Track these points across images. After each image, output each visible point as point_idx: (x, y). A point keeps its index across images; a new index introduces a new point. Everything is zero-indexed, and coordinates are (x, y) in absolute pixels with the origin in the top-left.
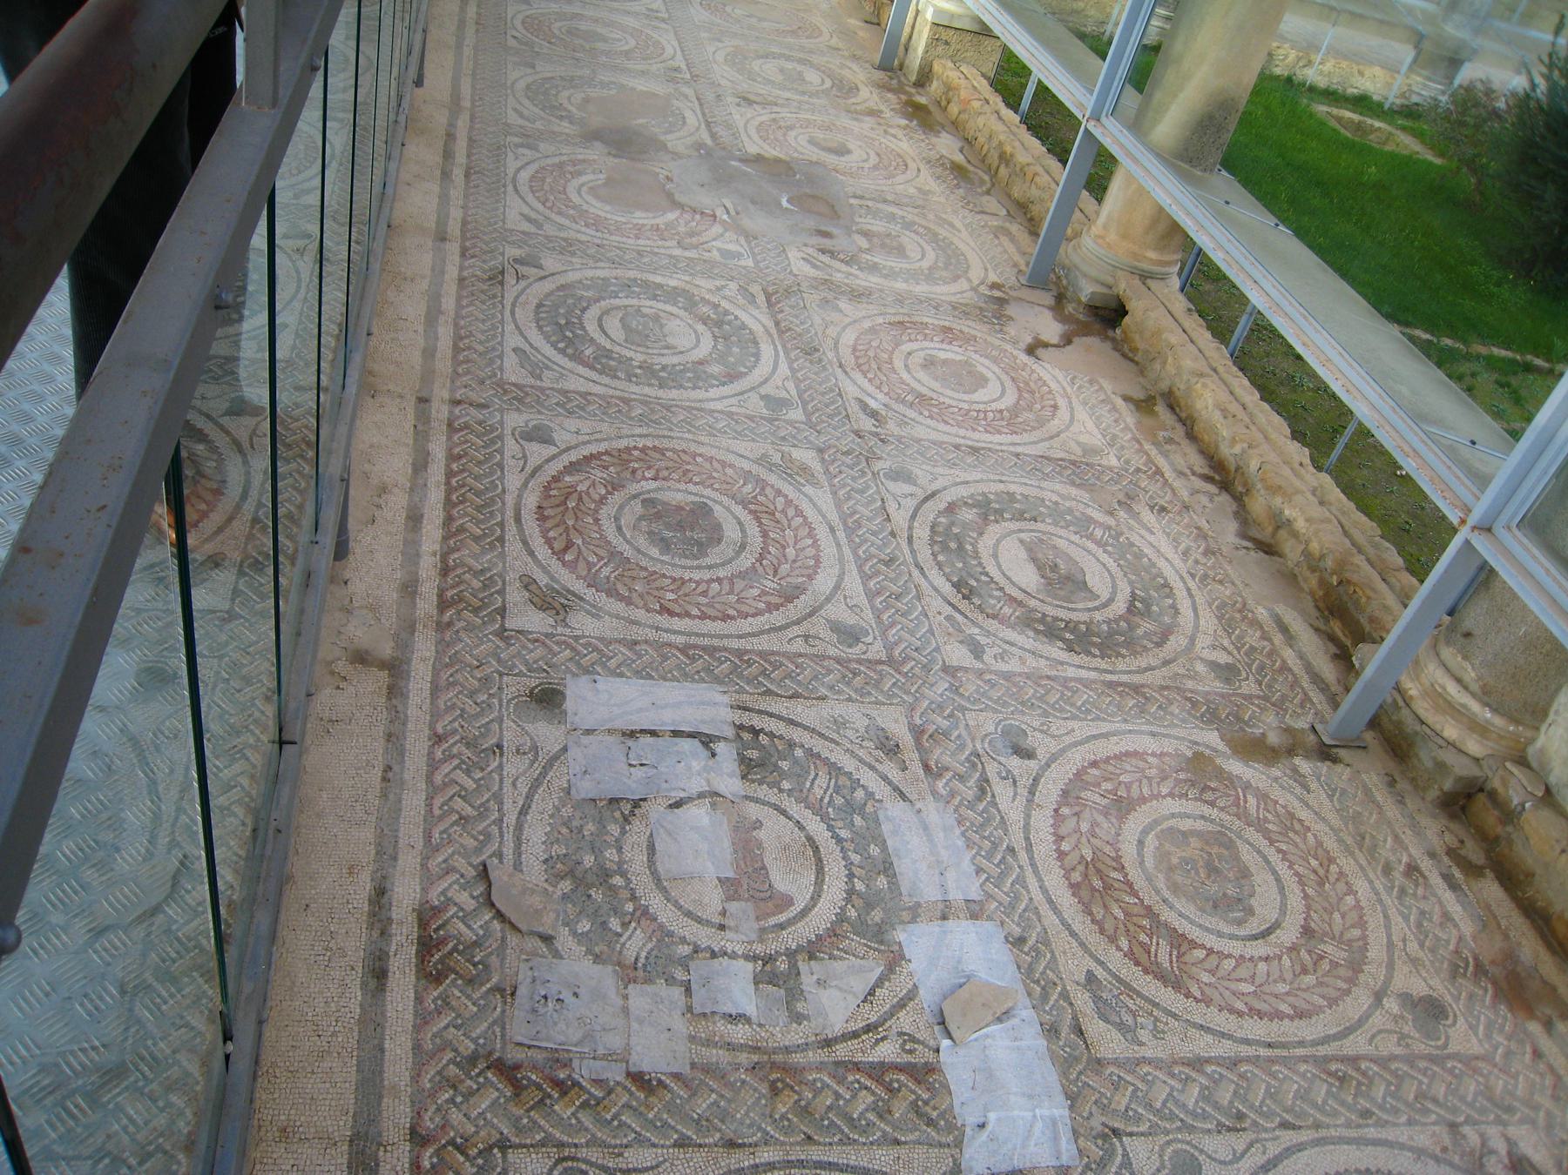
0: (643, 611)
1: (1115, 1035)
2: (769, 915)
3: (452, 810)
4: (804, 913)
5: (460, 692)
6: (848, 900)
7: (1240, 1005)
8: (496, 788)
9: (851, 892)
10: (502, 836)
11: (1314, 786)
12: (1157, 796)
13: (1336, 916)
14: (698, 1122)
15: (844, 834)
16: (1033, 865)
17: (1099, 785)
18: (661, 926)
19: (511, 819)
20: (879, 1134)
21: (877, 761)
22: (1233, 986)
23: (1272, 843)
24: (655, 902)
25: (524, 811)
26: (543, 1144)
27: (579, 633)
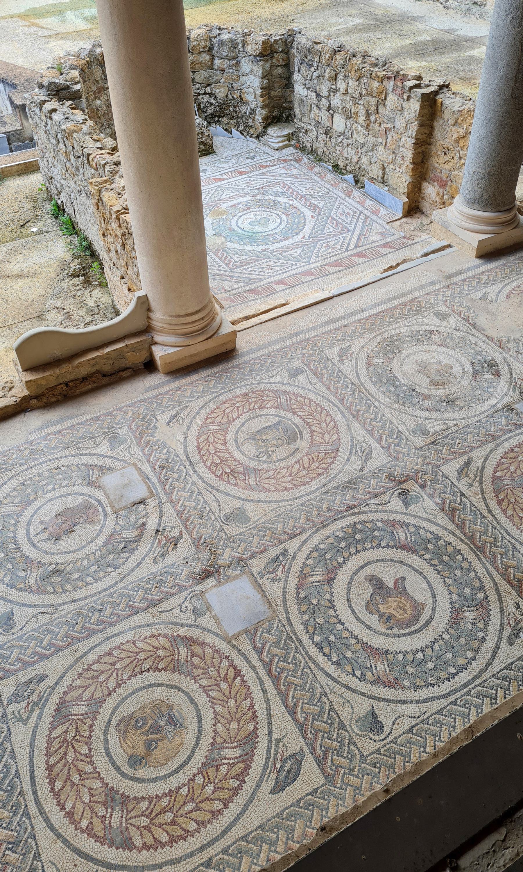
20: (10, 760)
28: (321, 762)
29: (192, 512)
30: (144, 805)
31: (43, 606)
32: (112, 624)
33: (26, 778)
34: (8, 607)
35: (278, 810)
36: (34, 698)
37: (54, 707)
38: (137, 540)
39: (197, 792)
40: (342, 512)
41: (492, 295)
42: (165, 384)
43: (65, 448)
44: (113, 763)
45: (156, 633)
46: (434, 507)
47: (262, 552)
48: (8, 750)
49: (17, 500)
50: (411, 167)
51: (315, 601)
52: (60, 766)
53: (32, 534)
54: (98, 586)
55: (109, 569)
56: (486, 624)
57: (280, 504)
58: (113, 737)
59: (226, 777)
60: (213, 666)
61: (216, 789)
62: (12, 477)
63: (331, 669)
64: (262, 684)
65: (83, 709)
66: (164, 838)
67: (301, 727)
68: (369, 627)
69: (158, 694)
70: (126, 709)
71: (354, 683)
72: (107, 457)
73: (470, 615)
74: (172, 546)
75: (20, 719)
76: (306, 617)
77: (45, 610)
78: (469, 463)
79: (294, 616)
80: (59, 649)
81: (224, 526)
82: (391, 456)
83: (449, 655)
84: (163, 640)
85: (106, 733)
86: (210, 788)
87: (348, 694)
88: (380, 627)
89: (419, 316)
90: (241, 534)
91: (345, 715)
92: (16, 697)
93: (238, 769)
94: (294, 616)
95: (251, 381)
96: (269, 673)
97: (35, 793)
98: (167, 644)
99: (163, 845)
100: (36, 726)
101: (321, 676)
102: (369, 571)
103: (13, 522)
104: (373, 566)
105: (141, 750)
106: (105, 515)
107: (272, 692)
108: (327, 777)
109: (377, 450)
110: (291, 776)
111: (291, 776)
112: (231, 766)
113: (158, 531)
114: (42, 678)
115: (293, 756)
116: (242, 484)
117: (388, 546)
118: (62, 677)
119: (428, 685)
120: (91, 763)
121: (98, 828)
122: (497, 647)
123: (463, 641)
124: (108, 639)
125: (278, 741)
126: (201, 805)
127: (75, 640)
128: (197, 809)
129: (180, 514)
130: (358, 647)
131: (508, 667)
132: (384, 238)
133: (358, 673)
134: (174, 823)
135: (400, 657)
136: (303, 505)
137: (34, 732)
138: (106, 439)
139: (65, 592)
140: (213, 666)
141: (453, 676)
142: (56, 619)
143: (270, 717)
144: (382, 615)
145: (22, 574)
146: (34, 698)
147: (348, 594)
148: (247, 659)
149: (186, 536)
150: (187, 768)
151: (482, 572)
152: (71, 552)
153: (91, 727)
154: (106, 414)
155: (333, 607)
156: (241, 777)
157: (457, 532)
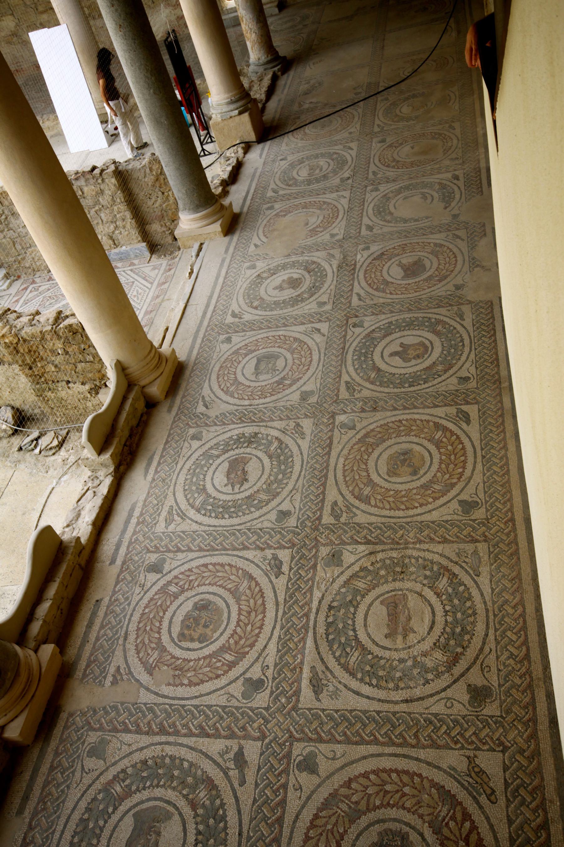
0: (424, 775)
1: (280, 556)
2: (391, 596)
3: (515, 634)
4: (378, 598)
5: (521, 702)
6: (359, 604)
7: (227, 568)
8: (498, 647)
9: (356, 607)
10: (494, 624)
11: (112, 670)
12: (199, 659)
13: (159, 604)
14: (428, 527)
15: (351, 633)
16: (276, 621)
17: (223, 665)
18: (432, 590)
19: (491, 632)
21: (324, 672)
22: (225, 575)
23: (160, 639)
24: (433, 599)
25: (487, 635)
26: (476, 520)
27: (462, 752)
28: (468, 403)
29: (285, 414)
30: (439, 474)
31: (288, 495)
32: (328, 466)
33: (389, 520)
34: (275, 512)
35: (478, 426)
36: (344, 509)
37: (357, 501)
38: (280, 442)
39: (448, 452)
40: (343, 352)
41: (259, 243)
42: (173, 402)
43: (177, 464)
44: (408, 482)
45: (350, 448)
46: (372, 317)
47: (339, 391)
48: (366, 525)
49: (196, 495)
50: (133, 221)
51: (386, 380)
52: (392, 505)
53: (231, 492)
54: (297, 468)
55: (290, 460)
56: (448, 324)
57: (315, 375)
58: (393, 479)
59: (449, 440)
60: (387, 430)
61: (452, 445)
62: (174, 495)
63: (426, 385)
64: (414, 413)
65: (369, 489)
66: (461, 470)
67: (445, 405)
68: (416, 365)
69: (385, 456)
70: (383, 469)
71: (440, 379)
72: (204, 444)
73: (439, 328)
74: (300, 429)
75: (352, 518)
76: (391, 386)
77: (292, 495)
78: (358, 295)
79: (386, 390)
80: (323, 493)
81: (309, 402)
82: (326, 322)
83: (453, 342)
84: (356, 447)
85: (390, 482)
86: (450, 448)
87: (443, 384)
88: (419, 361)
89: (242, 276)
90: (319, 397)
91: (452, 388)
92: (337, 517)
93: (448, 434)
94: (386, 390)
95: (213, 362)
96: (409, 409)
97: (399, 518)
98: (360, 445)
99: (464, 471)
100: (362, 511)
101: (427, 390)
102: (386, 354)
103: (211, 500)
104: (385, 351)
105: (410, 470)
106: (249, 454)
107: (420, 411)
108: (476, 403)
109: (317, 326)
110: (466, 415)
111: (466, 415)
112: (445, 437)
113: (284, 432)
114: (335, 503)
115: (457, 413)
116: (285, 387)
117: (379, 343)
118: (342, 494)
119: (461, 355)
120: (401, 491)
121: (437, 495)
122: (462, 325)
123: (449, 335)
124: (335, 470)
125: (446, 415)
126: (455, 452)
127: (324, 485)
128: (455, 455)
129: (281, 419)
130: (423, 372)
131: (474, 325)
132: (159, 270)
133: (436, 376)
134: (456, 465)
135: (440, 359)
136: (324, 366)
137: (364, 512)
138: (190, 441)
139: (287, 483)
140: (387, 430)
141: (463, 345)
142: (302, 491)
143: (431, 415)
144: (414, 358)
145: (256, 502)
146: (344, 509)
147: (392, 366)
148: (394, 416)
149: (299, 421)
150: (433, 454)
151: (421, 315)
152: (261, 476)
153: (381, 487)
154: (168, 436)
155: (394, 374)
156: (452, 433)
157: (394, 314)
